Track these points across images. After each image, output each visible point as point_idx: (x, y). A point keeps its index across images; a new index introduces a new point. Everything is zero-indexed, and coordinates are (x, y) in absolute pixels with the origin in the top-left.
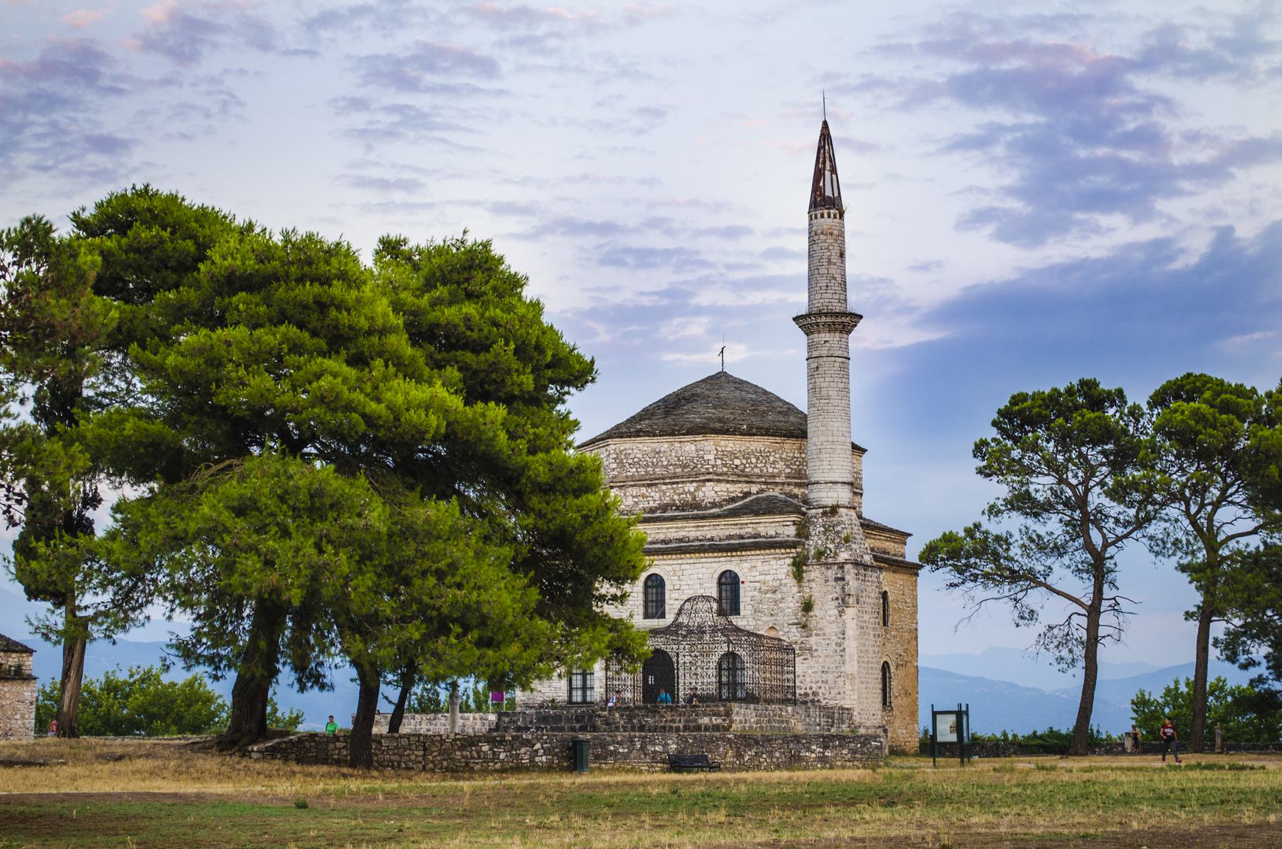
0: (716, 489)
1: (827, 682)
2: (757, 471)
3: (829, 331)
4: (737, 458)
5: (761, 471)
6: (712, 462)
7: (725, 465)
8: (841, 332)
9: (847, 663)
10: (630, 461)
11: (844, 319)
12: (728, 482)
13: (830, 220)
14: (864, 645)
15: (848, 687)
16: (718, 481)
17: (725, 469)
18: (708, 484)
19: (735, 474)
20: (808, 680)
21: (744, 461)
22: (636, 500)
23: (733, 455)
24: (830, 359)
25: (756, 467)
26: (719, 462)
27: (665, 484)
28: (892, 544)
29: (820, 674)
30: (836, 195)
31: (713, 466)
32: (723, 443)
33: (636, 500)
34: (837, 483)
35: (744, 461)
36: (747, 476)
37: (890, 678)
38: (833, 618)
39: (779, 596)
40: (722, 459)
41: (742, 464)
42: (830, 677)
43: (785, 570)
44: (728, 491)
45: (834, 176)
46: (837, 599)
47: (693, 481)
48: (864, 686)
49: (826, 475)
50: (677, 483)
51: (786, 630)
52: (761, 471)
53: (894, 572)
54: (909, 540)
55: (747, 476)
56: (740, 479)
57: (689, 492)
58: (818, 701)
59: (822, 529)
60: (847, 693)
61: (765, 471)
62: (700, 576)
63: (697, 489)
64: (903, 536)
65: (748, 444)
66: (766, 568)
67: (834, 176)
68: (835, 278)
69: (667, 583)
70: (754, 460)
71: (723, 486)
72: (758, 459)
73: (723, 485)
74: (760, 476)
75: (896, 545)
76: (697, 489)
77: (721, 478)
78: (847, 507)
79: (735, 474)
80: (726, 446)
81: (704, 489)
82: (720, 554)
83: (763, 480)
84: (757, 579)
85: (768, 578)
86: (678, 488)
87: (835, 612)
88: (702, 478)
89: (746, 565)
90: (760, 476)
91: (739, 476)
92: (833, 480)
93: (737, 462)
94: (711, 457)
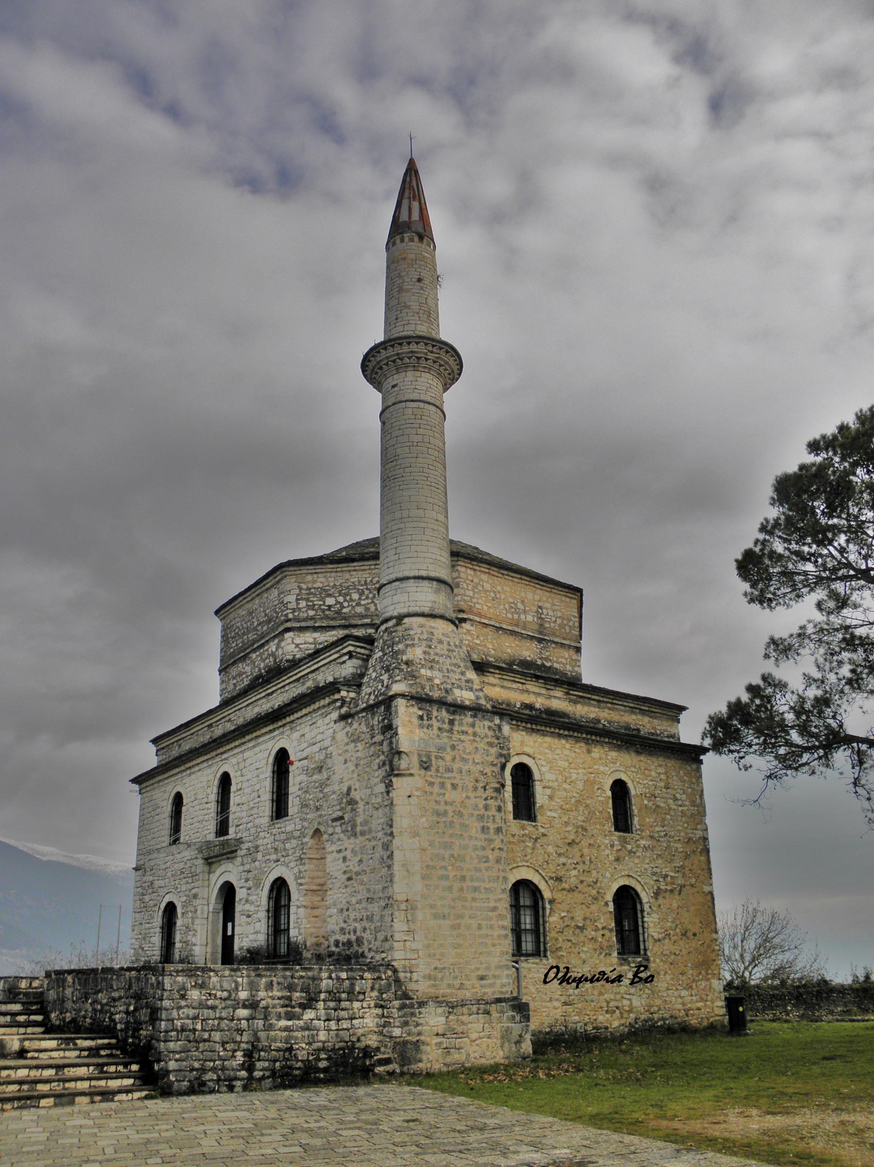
0: (298, 641)
1: (370, 919)
2: (359, 610)
3: (398, 371)
4: (330, 596)
5: (367, 609)
6: (293, 605)
7: (312, 607)
8: (415, 368)
9: (396, 879)
10: (233, 634)
11: (413, 347)
12: (315, 629)
13: (404, 244)
14: (446, 846)
15: (399, 925)
16: (301, 629)
17: (311, 613)
18: (288, 635)
19: (327, 618)
20: (352, 916)
21: (341, 599)
22: (235, 681)
23: (325, 592)
24: (397, 406)
25: (358, 604)
26: (303, 604)
27: (254, 651)
28: (646, 719)
29: (364, 904)
30: (416, 216)
31: (294, 610)
32: (309, 578)
33: (235, 681)
34: (407, 578)
35: (341, 599)
36: (345, 618)
37: (642, 911)
38: (379, 800)
39: (325, 775)
40: (307, 600)
41: (338, 602)
42: (375, 908)
43: (331, 731)
44: (315, 643)
45: (415, 205)
46: (384, 764)
47: (275, 637)
48: (447, 923)
49: (391, 570)
50: (263, 645)
51: (330, 831)
52: (367, 609)
53: (638, 753)
54: (683, 716)
55: (345, 618)
56: (332, 623)
57: (273, 654)
58: (363, 955)
59: (380, 654)
60: (397, 937)
61: (372, 608)
62: (258, 765)
63: (278, 646)
64: (674, 711)
65: (347, 576)
66: (313, 734)
67: (415, 205)
68: (409, 307)
69: (233, 781)
70: (355, 596)
71: (309, 637)
72: (361, 593)
73: (308, 634)
74: (366, 617)
75: (656, 722)
76: (278, 646)
77: (303, 624)
78: (423, 615)
79: (327, 618)
80: (314, 582)
81: (283, 644)
82: (271, 727)
83: (368, 621)
84: (304, 754)
85: (316, 748)
86: (263, 653)
87: (381, 788)
88: (281, 629)
89: (296, 735)
90: (363, 617)
91: (333, 619)
92: (400, 575)
93: (330, 601)
94: (292, 598)
